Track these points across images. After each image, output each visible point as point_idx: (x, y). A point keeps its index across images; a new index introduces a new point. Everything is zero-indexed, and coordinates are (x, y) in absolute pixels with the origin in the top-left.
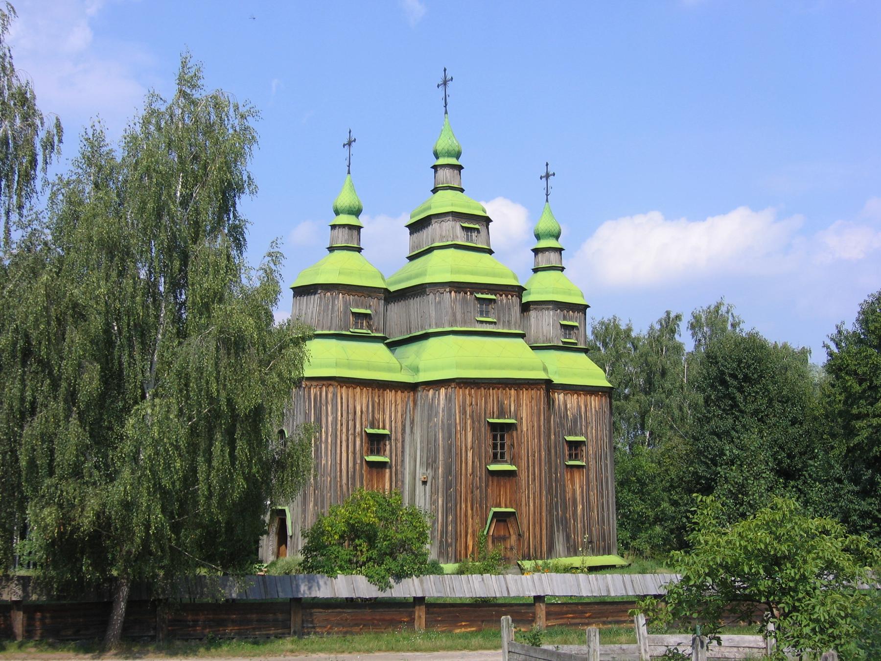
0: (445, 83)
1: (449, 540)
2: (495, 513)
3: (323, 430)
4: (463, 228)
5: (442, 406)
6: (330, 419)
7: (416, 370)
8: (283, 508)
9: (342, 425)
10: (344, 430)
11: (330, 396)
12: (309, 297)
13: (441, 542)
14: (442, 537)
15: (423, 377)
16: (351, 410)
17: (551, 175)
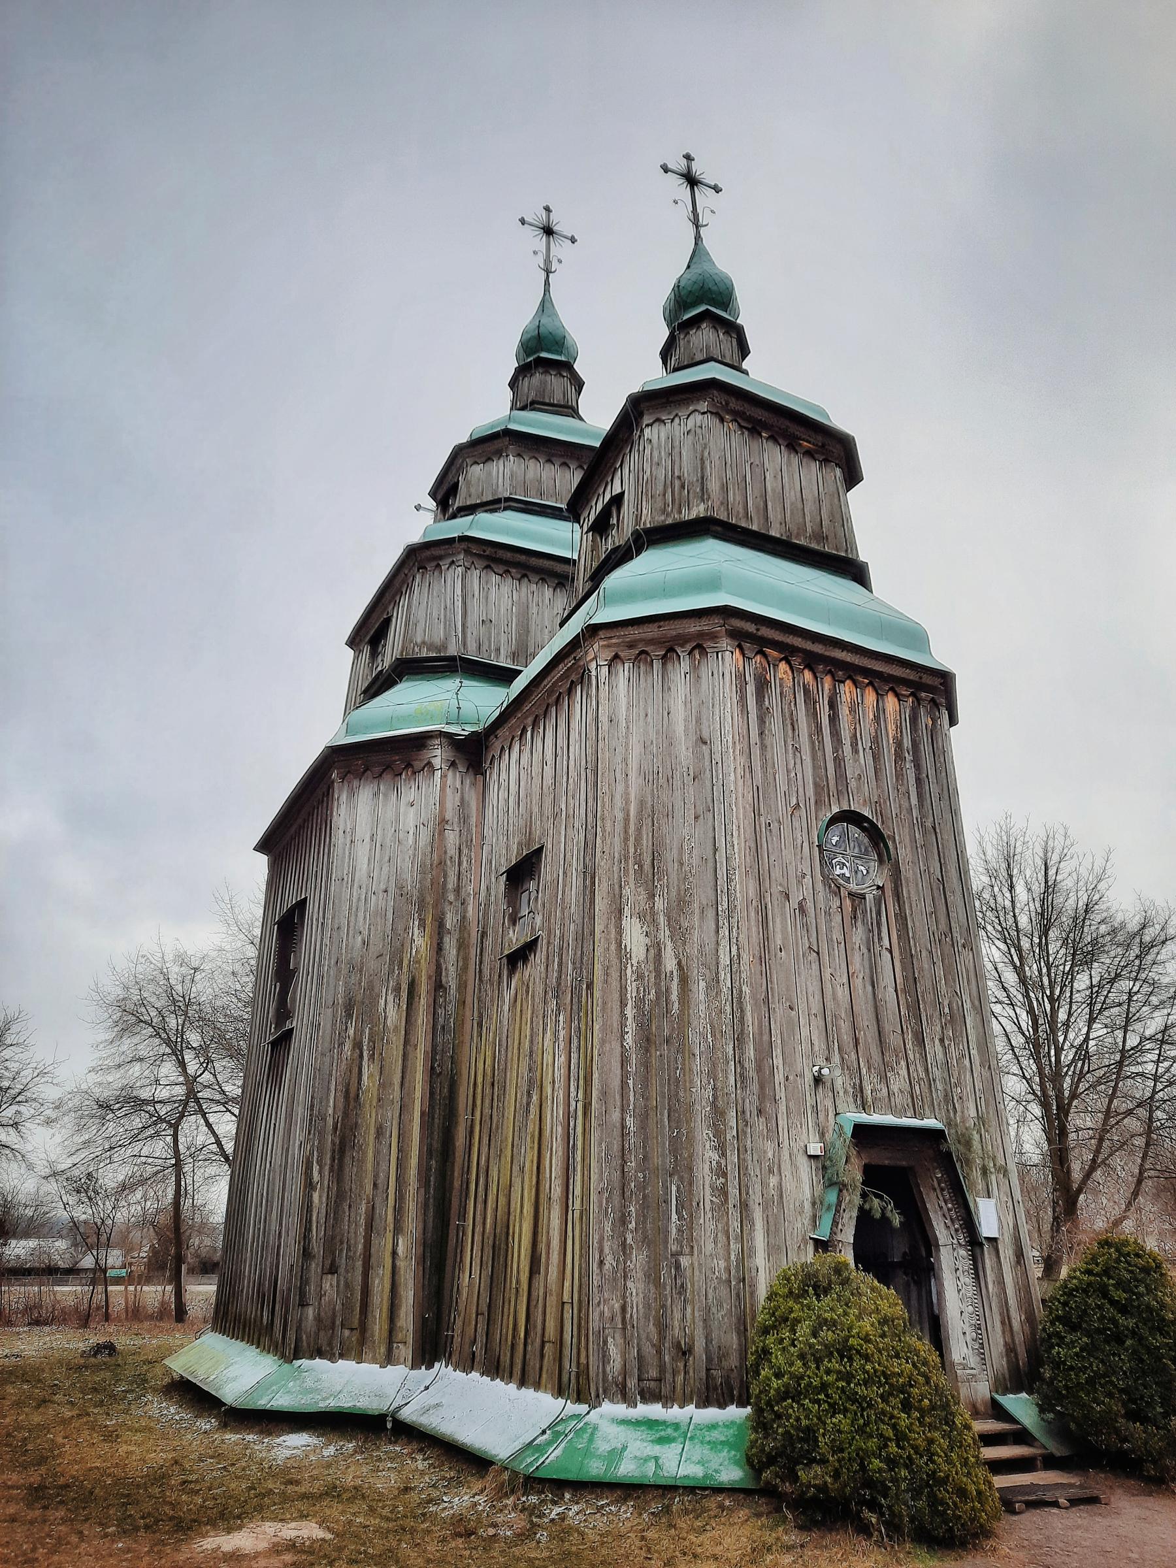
0: (548, 231)
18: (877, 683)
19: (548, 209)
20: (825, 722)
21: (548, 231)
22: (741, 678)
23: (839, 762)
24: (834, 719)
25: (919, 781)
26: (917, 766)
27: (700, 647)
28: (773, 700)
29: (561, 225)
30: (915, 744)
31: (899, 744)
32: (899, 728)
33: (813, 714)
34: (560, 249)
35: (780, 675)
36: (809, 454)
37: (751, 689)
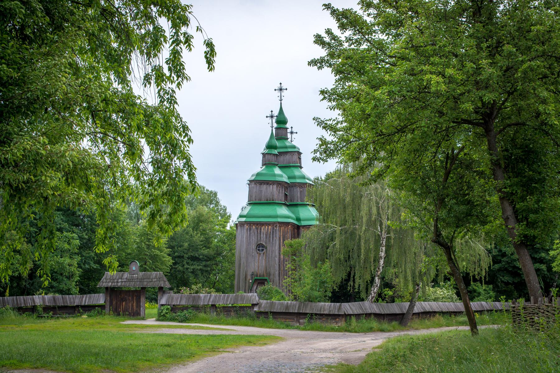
0: (281, 90)
7: (298, 219)
15: (303, 223)
19: (281, 84)
20: (259, 232)
21: (281, 90)
22: (247, 229)
23: (260, 237)
24: (260, 232)
25: (273, 237)
26: (273, 235)
27: (244, 225)
28: (252, 232)
29: (284, 87)
30: (273, 232)
31: (270, 232)
33: (257, 231)
34: (284, 93)
36: (271, 184)
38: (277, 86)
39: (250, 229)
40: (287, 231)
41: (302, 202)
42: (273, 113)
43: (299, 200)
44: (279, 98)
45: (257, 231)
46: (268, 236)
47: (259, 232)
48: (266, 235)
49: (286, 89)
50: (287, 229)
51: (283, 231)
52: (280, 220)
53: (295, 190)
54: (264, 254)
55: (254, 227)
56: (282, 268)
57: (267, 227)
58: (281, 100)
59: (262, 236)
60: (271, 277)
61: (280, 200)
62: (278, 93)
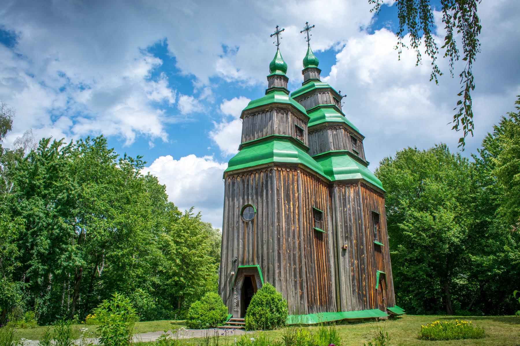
0: (307, 29)
1: (364, 292)
2: (381, 274)
3: (291, 203)
4: (334, 98)
5: (353, 197)
6: (296, 195)
7: (331, 173)
8: (256, 266)
9: (303, 201)
10: (304, 206)
11: (296, 177)
12: (264, 115)
13: (359, 294)
14: (359, 290)
15: (338, 177)
16: (307, 192)
17: (344, 96)
18: (258, 171)
20: (246, 186)
24: (248, 185)
29: (310, 25)
31: (263, 183)
32: (263, 179)
33: (244, 186)
35: (238, 180)
36: (268, 111)
37: (231, 186)
38: (303, 26)
39: (234, 184)
40: (293, 178)
41: (337, 149)
42: (279, 28)
43: (332, 148)
44: (307, 39)
45: (244, 186)
46: (259, 190)
47: (246, 186)
48: (256, 189)
49: (314, 26)
50: (293, 175)
51: (284, 179)
52: (276, 159)
53: (325, 134)
54: (253, 222)
55: (239, 179)
56: (284, 245)
57: (257, 175)
58: (308, 41)
59: (250, 191)
60: (265, 263)
61: (284, 133)
62: (305, 34)
